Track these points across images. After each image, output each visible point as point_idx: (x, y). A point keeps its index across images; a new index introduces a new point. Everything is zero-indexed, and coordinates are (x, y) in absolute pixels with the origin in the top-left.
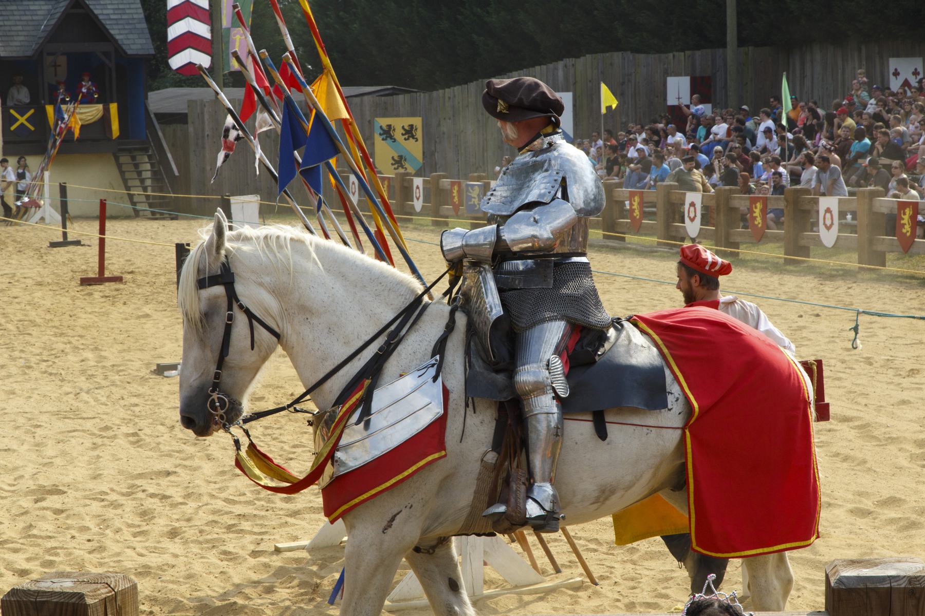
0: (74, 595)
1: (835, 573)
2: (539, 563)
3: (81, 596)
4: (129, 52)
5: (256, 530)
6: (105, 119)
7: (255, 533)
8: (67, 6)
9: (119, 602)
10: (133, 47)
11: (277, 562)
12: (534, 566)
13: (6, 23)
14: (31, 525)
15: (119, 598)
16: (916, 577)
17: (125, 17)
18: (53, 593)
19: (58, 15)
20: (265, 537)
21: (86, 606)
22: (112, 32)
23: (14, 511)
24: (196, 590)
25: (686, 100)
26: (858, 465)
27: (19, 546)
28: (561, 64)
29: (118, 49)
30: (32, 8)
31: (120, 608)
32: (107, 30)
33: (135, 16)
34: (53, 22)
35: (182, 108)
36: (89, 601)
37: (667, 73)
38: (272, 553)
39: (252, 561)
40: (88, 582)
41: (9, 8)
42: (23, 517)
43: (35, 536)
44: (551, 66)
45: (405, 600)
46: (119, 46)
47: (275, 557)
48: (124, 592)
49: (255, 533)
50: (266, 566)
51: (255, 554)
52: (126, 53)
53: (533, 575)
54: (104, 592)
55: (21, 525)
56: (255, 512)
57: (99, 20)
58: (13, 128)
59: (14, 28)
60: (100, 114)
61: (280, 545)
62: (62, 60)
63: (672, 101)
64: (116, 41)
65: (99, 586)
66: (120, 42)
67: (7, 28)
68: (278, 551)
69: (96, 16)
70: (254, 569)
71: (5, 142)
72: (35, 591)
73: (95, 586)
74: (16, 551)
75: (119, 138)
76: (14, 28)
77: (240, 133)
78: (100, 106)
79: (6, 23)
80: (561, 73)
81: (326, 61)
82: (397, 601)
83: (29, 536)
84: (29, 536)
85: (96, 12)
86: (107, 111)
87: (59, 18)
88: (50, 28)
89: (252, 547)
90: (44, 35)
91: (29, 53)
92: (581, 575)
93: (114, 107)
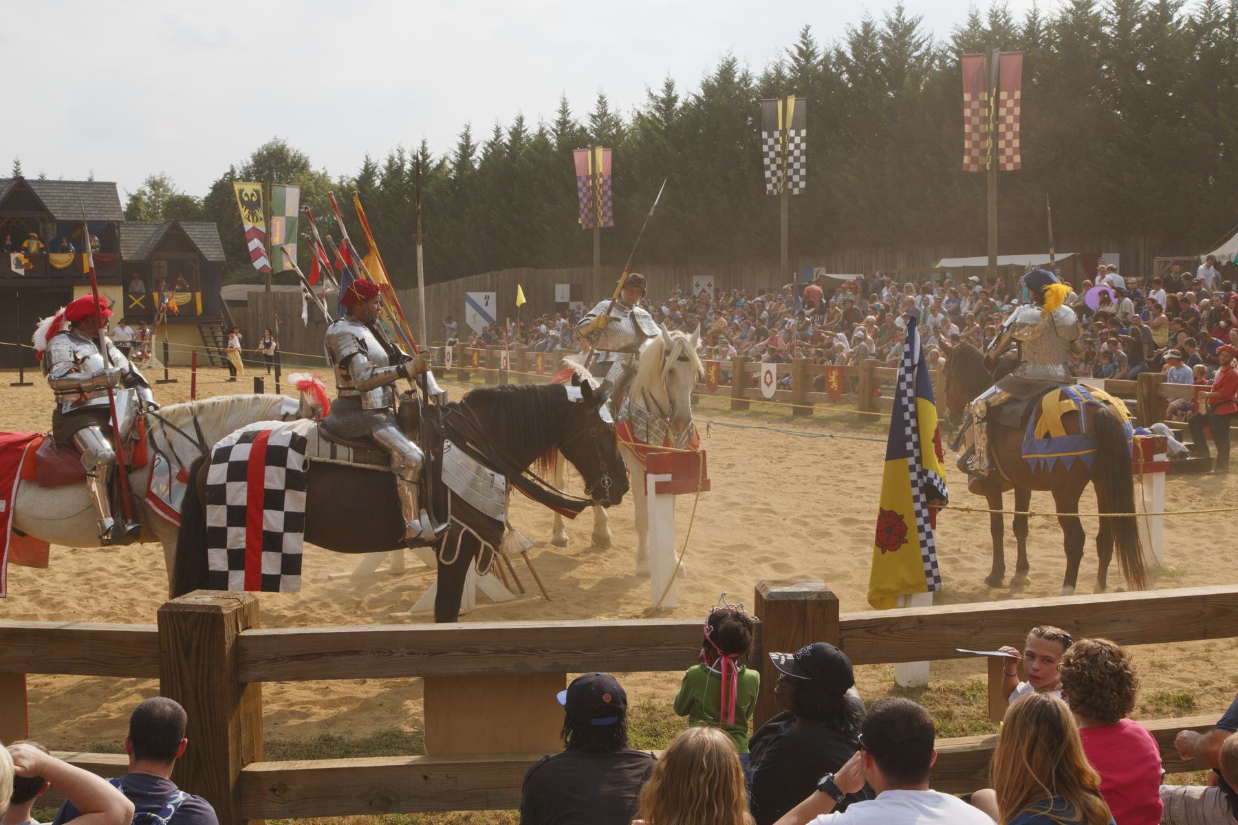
0: (214, 607)
1: (765, 590)
2: (510, 585)
3: (218, 608)
4: (209, 260)
5: (314, 565)
6: (192, 304)
7: (314, 567)
9: (246, 612)
11: (330, 586)
12: (507, 586)
14: (155, 562)
15: (246, 609)
16: (823, 593)
18: (197, 606)
19: (161, 235)
20: (321, 570)
21: (222, 615)
22: (198, 246)
23: (142, 552)
24: (276, 606)
25: (567, 299)
26: (709, 523)
27: (147, 576)
28: (489, 275)
29: (202, 258)
31: (247, 617)
34: (159, 238)
35: (244, 297)
36: (225, 612)
37: (555, 282)
38: (326, 581)
39: (313, 586)
40: (223, 598)
42: (150, 557)
43: (159, 569)
44: (483, 275)
45: (422, 612)
47: (328, 583)
48: (249, 605)
49: (314, 567)
50: (323, 589)
51: (314, 581)
53: (508, 595)
54: (235, 605)
55: (148, 562)
56: (312, 553)
58: (130, 307)
60: (189, 299)
61: (332, 575)
62: (164, 264)
63: (558, 299)
64: (200, 252)
65: (232, 600)
68: (330, 579)
69: (188, 236)
70: (314, 591)
72: (183, 605)
73: (229, 601)
74: (146, 579)
75: (201, 315)
77: (309, 294)
78: (190, 294)
80: (488, 279)
81: (373, 244)
82: (418, 612)
83: (155, 569)
84: (155, 569)
86: (194, 297)
89: (312, 577)
91: (143, 258)
92: (539, 595)
93: (198, 295)
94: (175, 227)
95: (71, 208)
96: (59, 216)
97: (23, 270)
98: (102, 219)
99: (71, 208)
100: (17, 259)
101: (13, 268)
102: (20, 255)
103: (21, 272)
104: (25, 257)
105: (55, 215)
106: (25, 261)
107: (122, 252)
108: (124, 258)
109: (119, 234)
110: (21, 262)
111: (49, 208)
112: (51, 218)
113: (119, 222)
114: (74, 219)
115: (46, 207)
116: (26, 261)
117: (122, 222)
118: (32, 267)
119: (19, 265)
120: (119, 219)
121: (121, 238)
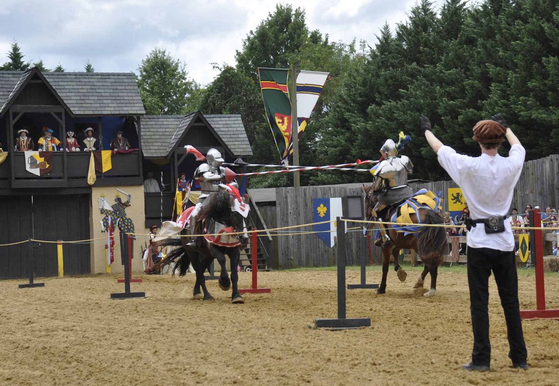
8: (191, 120)
10: (237, 150)
13: (148, 133)
17: (230, 129)
19: (185, 127)
22: (223, 139)
30: (165, 123)
32: (218, 135)
33: (238, 129)
34: (182, 132)
41: (149, 123)
46: (229, 150)
52: (233, 154)
57: (215, 132)
59: (153, 137)
64: (226, 146)
66: (229, 147)
67: (149, 137)
69: (213, 129)
71: (147, 218)
76: (153, 137)
79: (148, 133)
85: (213, 126)
87: (186, 129)
88: (179, 136)
90: (176, 141)
94: (199, 119)
95: (87, 101)
96: (76, 110)
97: (38, 170)
98: (122, 112)
99: (87, 101)
100: (32, 157)
101: (28, 168)
102: (36, 154)
103: (36, 172)
104: (41, 155)
105: (72, 109)
106: (40, 160)
107: (143, 148)
108: (145, 155)
109: (139, 128)
110: (37, 161)
111: (65, 102)
112: (68, 112)
113: (139, 116)
114: (91, 113)
115: (62, 101)
116: (42, 159)
117: (142, 115)
118: (48, 166)
119: (34, 163)
120: (139, 112)
121: (142, 133)
